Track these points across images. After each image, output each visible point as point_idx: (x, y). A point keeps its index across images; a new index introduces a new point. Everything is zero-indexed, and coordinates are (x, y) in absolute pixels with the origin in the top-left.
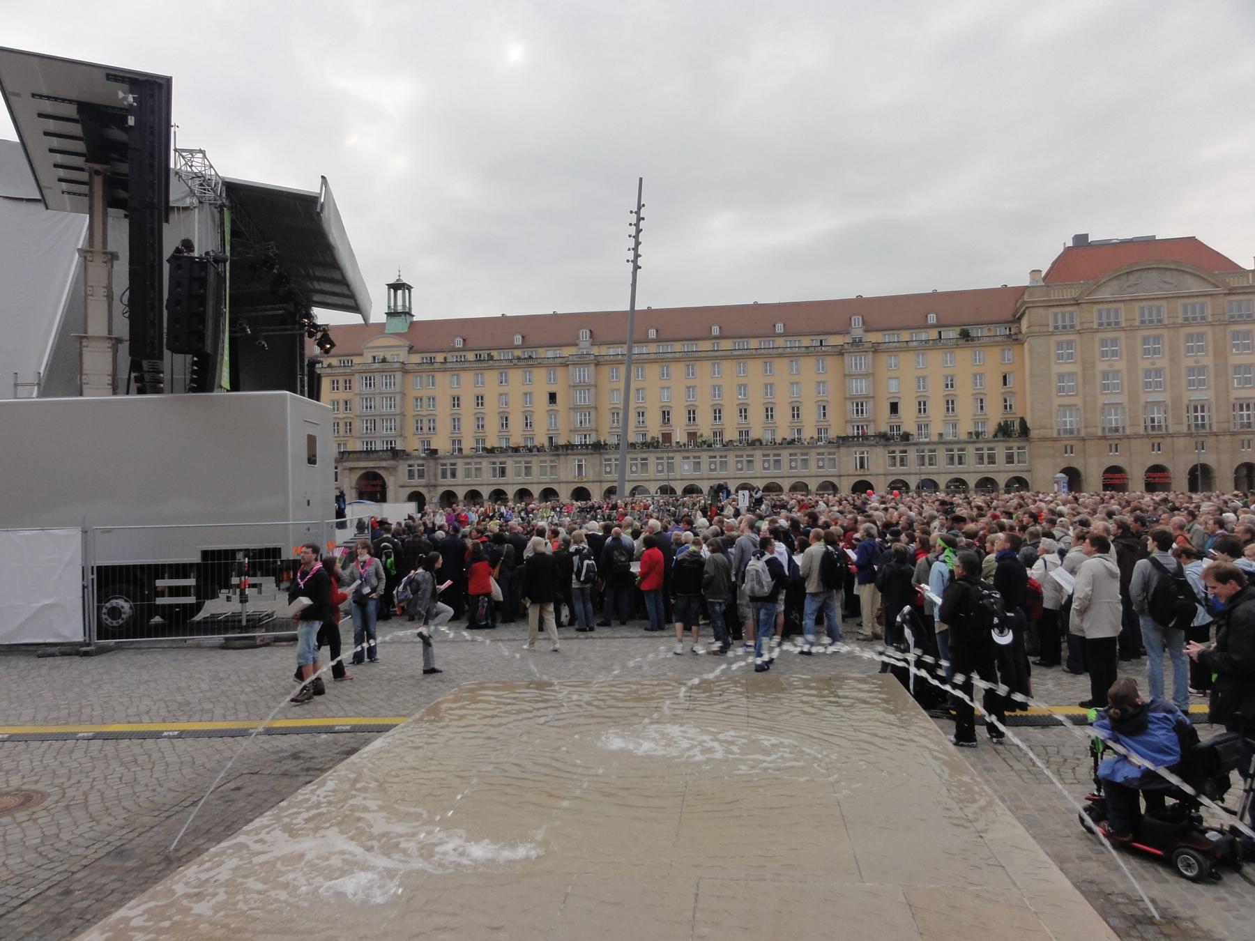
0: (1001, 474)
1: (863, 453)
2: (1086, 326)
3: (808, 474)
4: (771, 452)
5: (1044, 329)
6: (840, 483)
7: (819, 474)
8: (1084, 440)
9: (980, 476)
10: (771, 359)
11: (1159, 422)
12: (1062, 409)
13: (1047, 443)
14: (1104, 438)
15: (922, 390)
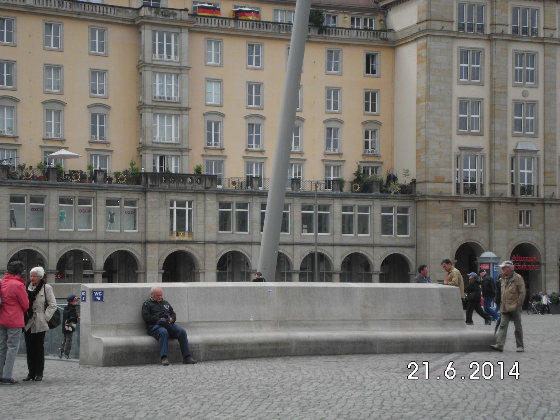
0: (377, 249)
1: (405, 210)
2: (499, 29)
3: (92, 237)
4: (28, 193)
5: (447, 27)
6: (145, 255)
7: (109, 238)
8: (489, 202)
9: (349, 251)
10: (13, 15)
11: (473, 180)
12: (463, 153)
13: (443, 204)
14: (515, 201)
15: (254, 106)
